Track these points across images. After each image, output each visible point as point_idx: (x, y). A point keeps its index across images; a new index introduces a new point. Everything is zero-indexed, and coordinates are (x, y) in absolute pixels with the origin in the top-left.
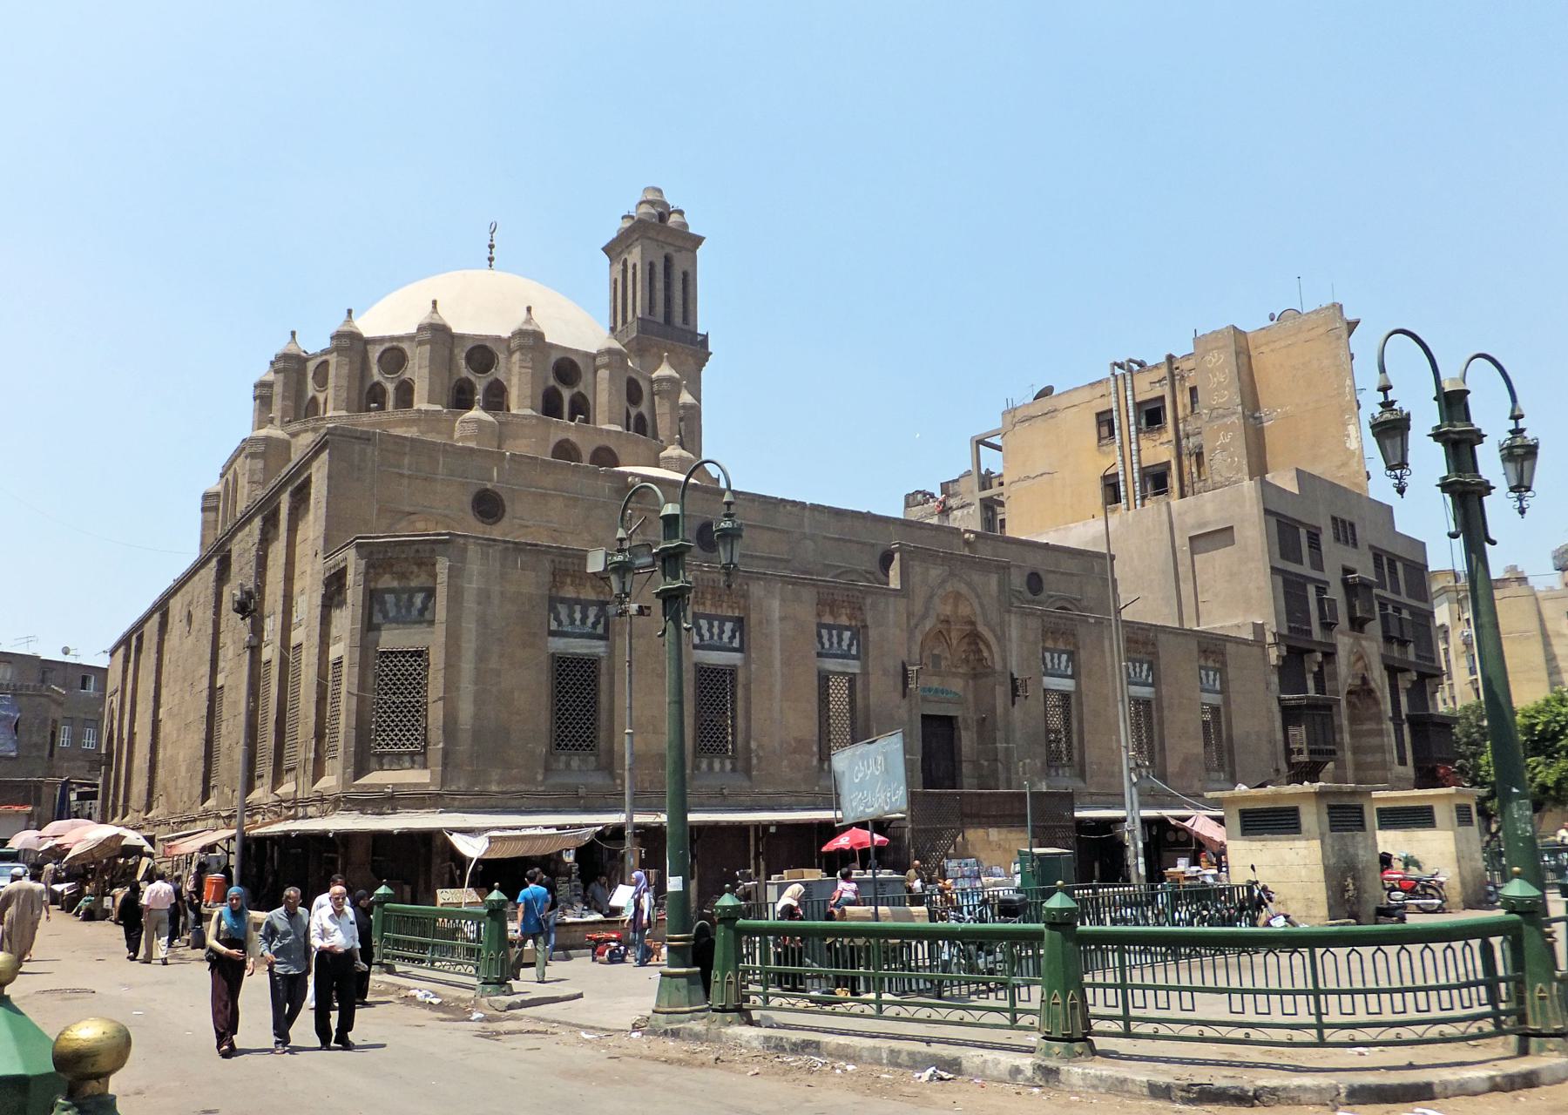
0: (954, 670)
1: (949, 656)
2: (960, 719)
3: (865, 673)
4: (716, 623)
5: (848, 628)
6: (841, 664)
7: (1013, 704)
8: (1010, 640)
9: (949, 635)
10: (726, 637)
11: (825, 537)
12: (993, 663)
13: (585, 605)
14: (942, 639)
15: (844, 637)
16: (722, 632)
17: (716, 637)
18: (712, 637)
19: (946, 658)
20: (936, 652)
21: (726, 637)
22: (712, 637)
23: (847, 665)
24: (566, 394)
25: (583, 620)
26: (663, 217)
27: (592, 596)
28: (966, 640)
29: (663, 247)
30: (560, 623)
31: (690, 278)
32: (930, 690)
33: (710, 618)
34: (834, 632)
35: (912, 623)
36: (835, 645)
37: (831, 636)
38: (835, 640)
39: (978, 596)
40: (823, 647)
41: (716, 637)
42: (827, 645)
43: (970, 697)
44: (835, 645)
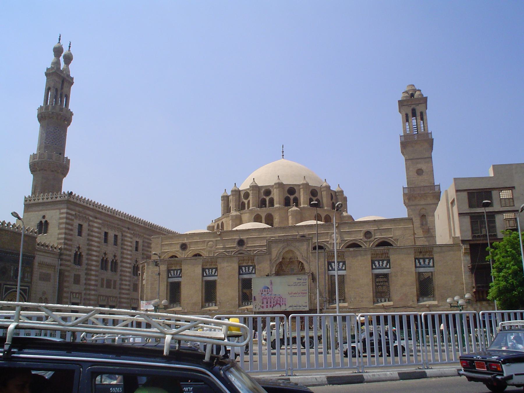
0: (299, 272)
4: (210, 270)
5: (251, 266)
10: (213, 273)
13: (177, 270)
16: (212, 272)
17: (210, 273)
18: (209, 273)
21: (213, 273)
22: (209, 273)
23: (251, 276)
24: (267, 199)
25: (177, 274)
26: (412, 95)
27: (178, 268)
29: (410, 107)
30: (171, 275)
31: (424, 114)
33: (209, 269)
38: (247, 269)
40: (243, 272)
41: (210, 273)
42: (244, 271)
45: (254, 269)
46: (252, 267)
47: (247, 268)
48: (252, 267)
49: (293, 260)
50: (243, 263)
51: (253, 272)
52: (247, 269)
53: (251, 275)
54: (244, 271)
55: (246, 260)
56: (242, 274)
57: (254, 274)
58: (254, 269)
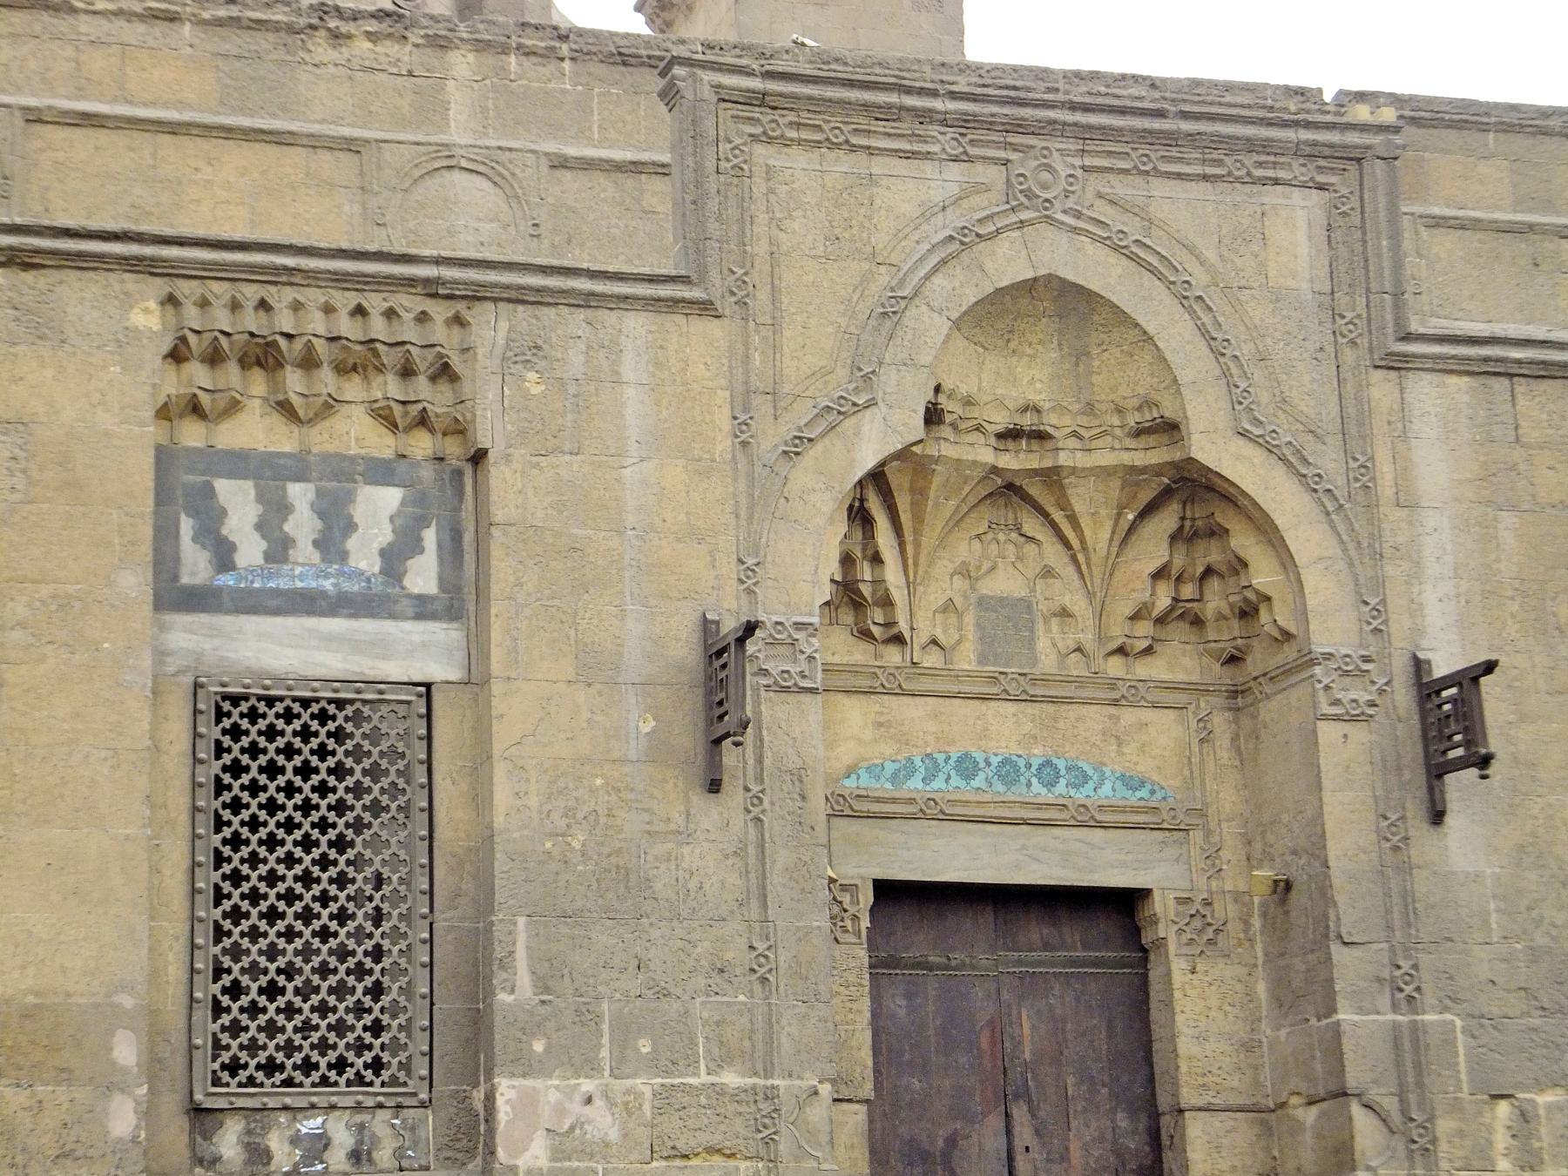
0: (1115, 667)
1: (1077, 602)
2: (1162, 904)
3: (476, 681)
5: (381, 472)
6: (329, 640)
7: (1437, 816)
8: (1407, 502)
9: (1064, 505)
11: (561, 164)
12: (1303, 614)
14: (1032, 525)
15: (359, 512)
19: (1064, 613)
20: (1005, 583)
23: (382, 648)
28: (1167, 521)
32: (967, 767)
34: (300, 494)
35: (771, 436)
36: (305, 551)
37: (275, 511)
38: (303, 524)
39: (1186, 298)
42: (250, 551)
43: (1226, 797)
44: (305, 551)
45: (430, 536)
46: (390, 498)
47: (300, 494)
48: (390, 498)
49: (1064, 459)
50: (233, 407)
51: (423, 576)
52: (303, 524)
53: (368, 626)
54: (250, 551)
55: (309, 362)
56: (197, 600)
57: (423, 609)
58: (430, 536)
